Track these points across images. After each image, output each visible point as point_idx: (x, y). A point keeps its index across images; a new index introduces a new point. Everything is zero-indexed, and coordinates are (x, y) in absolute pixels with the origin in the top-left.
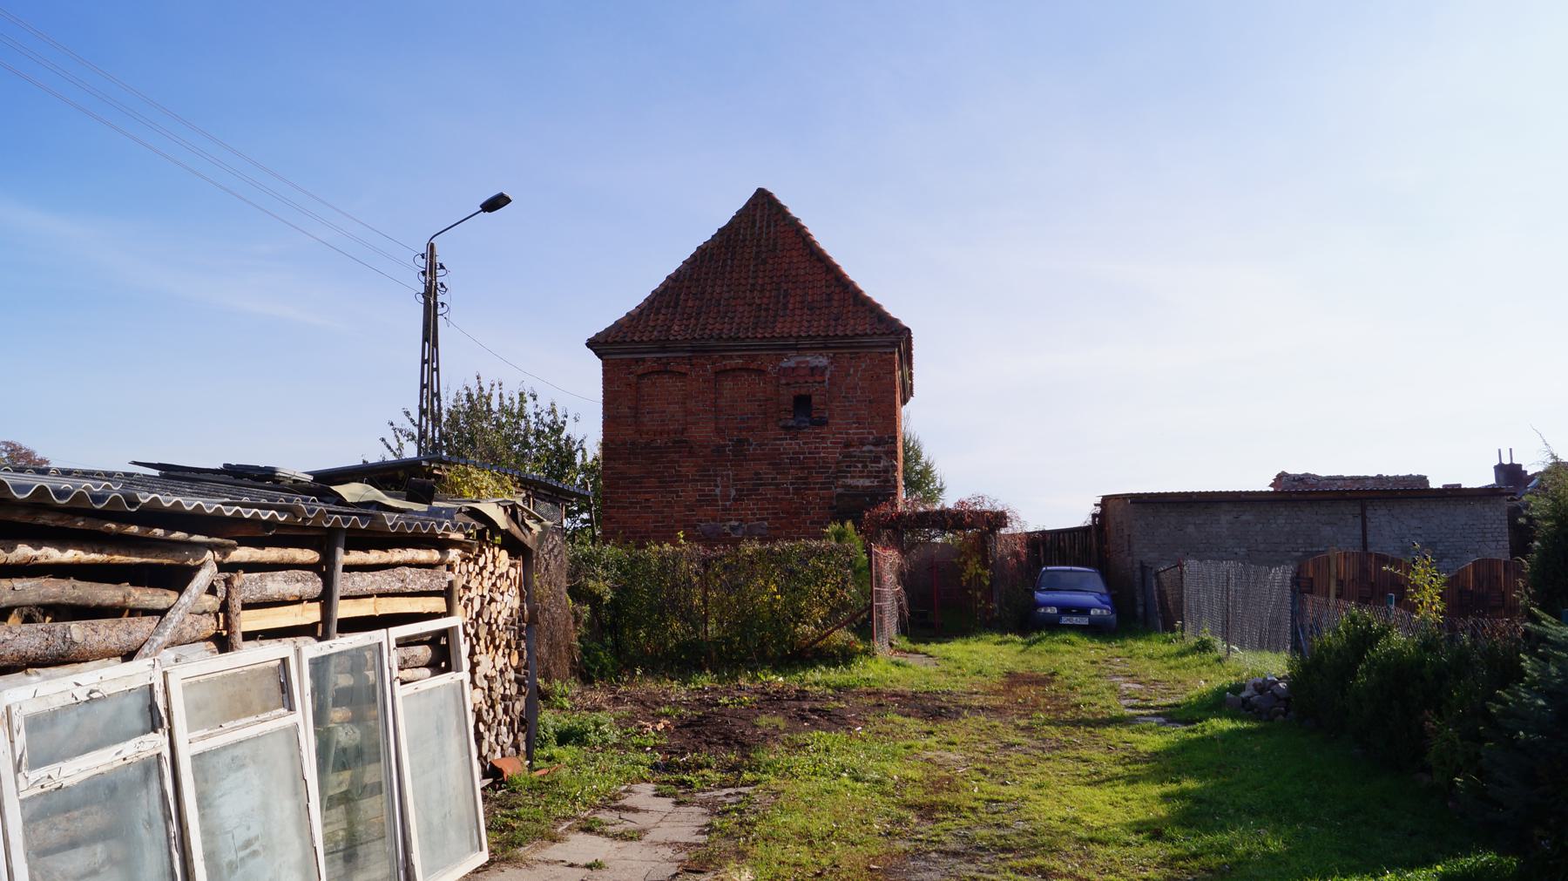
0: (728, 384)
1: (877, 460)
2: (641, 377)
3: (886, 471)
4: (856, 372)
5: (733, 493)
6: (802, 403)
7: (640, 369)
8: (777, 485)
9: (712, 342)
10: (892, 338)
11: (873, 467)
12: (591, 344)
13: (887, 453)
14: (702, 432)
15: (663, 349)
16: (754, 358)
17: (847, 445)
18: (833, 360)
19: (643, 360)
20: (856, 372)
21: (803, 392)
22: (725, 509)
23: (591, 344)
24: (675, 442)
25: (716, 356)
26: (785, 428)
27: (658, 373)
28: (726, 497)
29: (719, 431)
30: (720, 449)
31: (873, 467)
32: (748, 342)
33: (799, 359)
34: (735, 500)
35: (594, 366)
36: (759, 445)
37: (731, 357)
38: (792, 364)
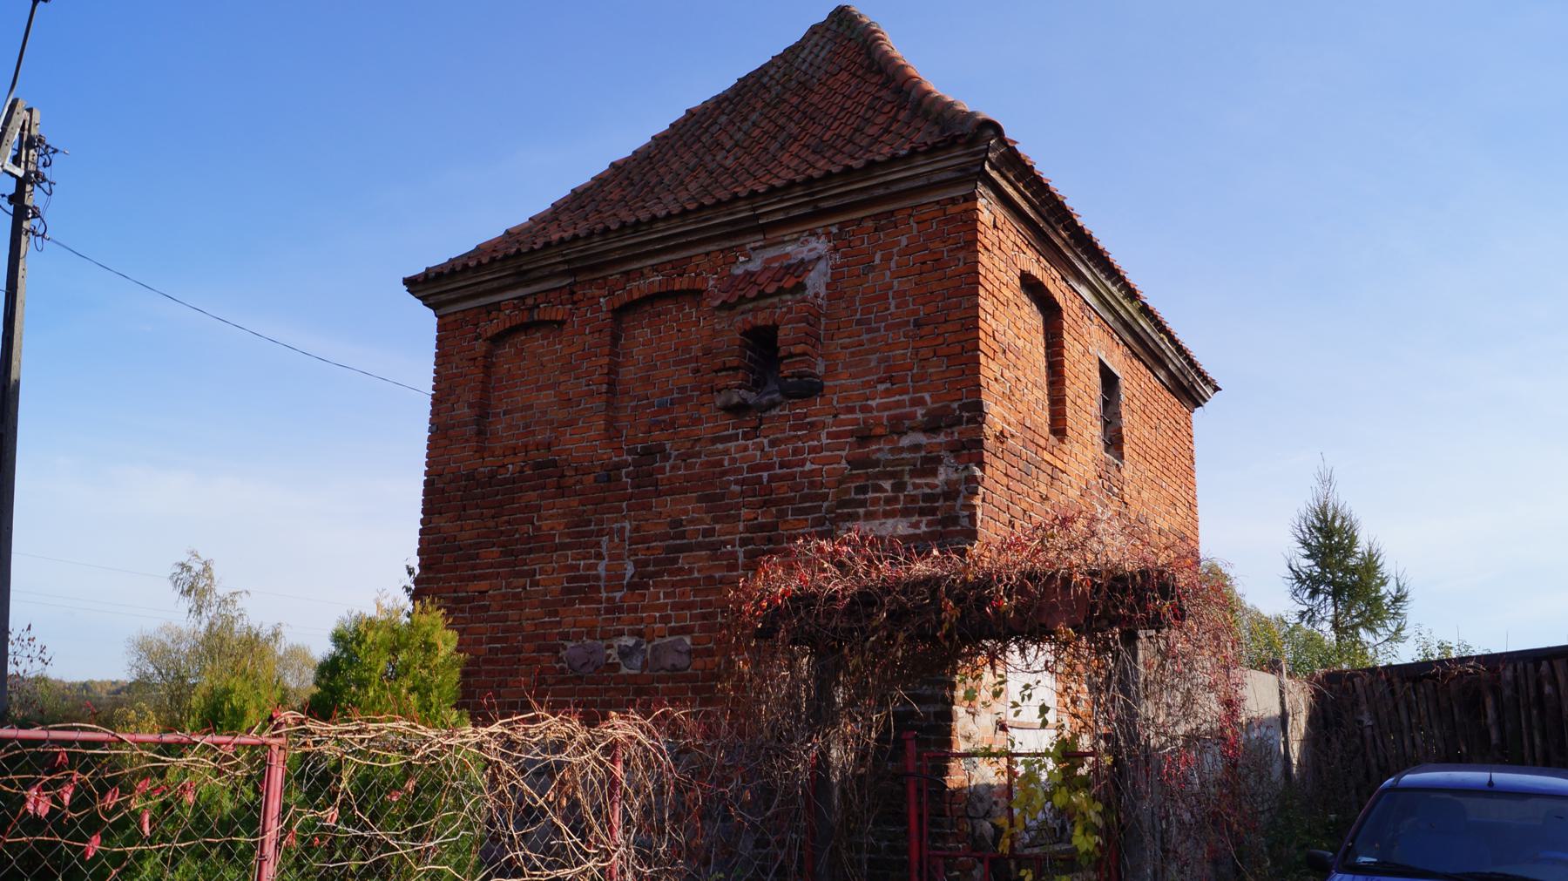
0: (641, 337)
1: (929, 466)
2: (498, 339)
3: (951, 493)
4: (887, 259)
5: (630, 569)
6: (762, 342)
7: (491, 329)
8: (714, 547)
9: (597, 245)
10: (958, 157)
11: (916, 486)
12: (412, 284)
13: (956, 449)
14: (584, 442)
15: (522, 278)
16: (680, 268)
17: (864, 438)
18: (839, 242)
19: (497, 306)
20: (887, 259)
21: (761, 319)
22: (613, 608)
23: (412, 284)
24: (538, 466)
25: (614, 274)
26: (729, 409)
27: (525, 328)
28: (615, 580)
29: (612, 433)
30: (610, 474)
31: (916, 486)
32: (661, 229)
33: (771, 253)
34: (632, 586)
35: (424, 322)
36: (684, 457)
37: (641, 273)
38: (755, 266)
